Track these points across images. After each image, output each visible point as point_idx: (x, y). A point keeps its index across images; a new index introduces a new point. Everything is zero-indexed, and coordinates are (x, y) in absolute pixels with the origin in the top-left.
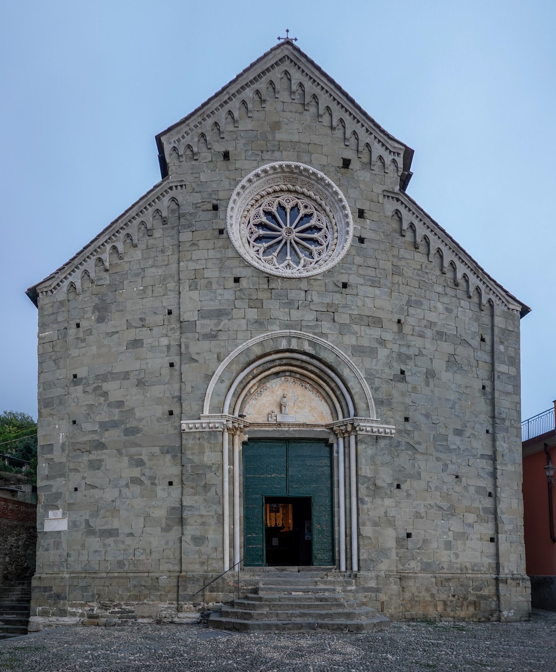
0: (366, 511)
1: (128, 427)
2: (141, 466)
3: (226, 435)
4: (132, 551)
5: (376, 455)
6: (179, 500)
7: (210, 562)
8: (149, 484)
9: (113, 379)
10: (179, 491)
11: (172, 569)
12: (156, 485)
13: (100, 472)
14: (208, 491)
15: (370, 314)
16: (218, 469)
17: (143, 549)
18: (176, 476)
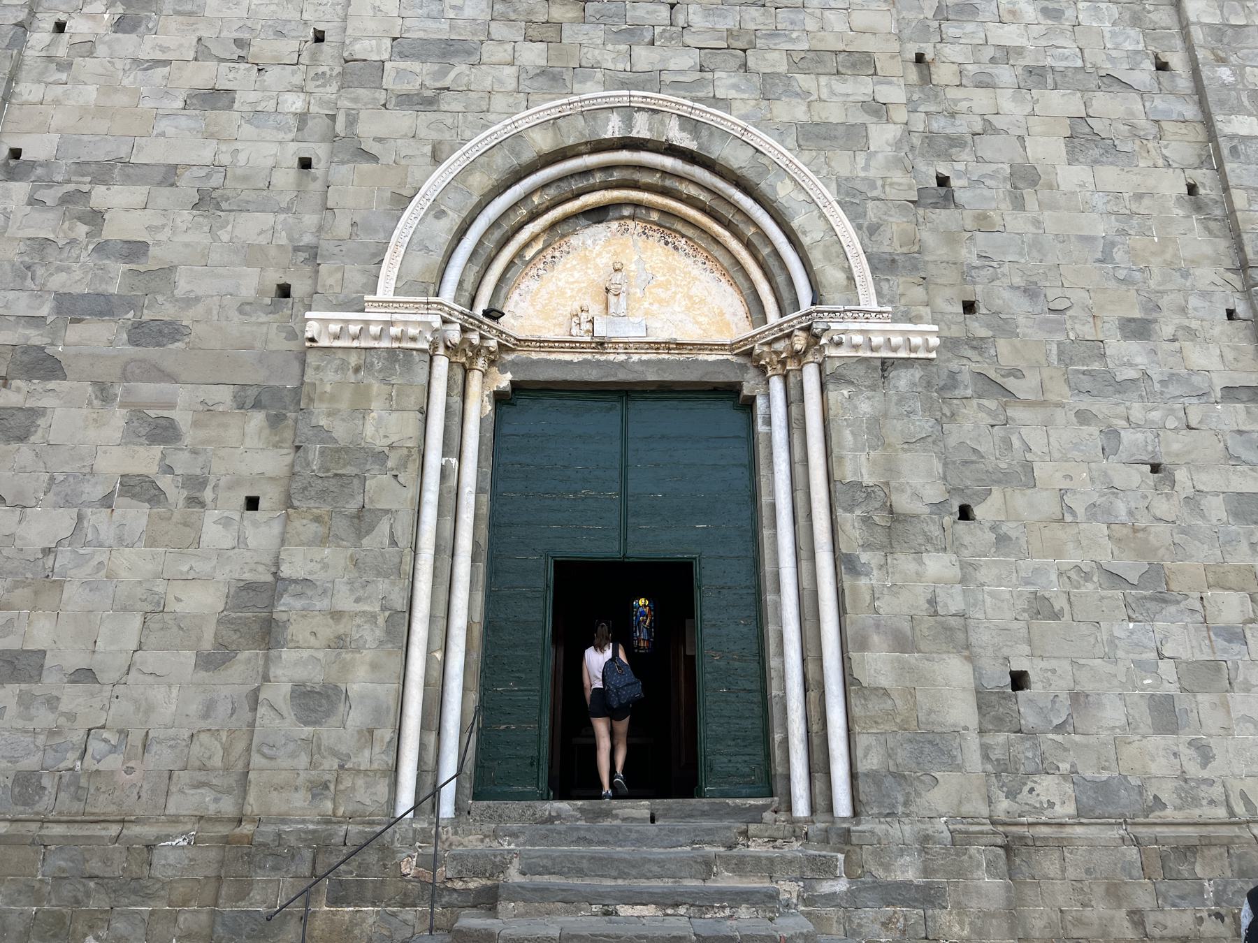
0: (868, 598)
1: (147, 316)
2: (165, 441)
3: (441, 364)
4: (77, 737)
5: (885, 415)
6: (268, 559)
7: (347, 782)
8: (181, 503)
9: (128, 180)
10: (276, 528)
11: (212, 809)
12: (202, 505)
13: (24, 448)
14: (368, 533)
15: (841, 47)
16: (403, 464)
17: (120, 732)
18: (272, 479)
